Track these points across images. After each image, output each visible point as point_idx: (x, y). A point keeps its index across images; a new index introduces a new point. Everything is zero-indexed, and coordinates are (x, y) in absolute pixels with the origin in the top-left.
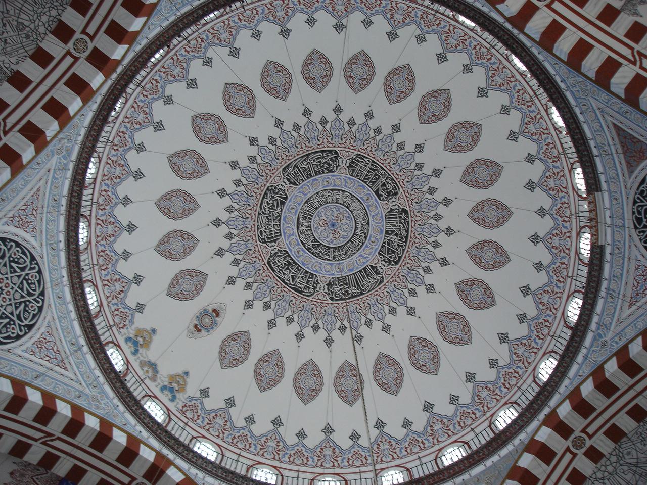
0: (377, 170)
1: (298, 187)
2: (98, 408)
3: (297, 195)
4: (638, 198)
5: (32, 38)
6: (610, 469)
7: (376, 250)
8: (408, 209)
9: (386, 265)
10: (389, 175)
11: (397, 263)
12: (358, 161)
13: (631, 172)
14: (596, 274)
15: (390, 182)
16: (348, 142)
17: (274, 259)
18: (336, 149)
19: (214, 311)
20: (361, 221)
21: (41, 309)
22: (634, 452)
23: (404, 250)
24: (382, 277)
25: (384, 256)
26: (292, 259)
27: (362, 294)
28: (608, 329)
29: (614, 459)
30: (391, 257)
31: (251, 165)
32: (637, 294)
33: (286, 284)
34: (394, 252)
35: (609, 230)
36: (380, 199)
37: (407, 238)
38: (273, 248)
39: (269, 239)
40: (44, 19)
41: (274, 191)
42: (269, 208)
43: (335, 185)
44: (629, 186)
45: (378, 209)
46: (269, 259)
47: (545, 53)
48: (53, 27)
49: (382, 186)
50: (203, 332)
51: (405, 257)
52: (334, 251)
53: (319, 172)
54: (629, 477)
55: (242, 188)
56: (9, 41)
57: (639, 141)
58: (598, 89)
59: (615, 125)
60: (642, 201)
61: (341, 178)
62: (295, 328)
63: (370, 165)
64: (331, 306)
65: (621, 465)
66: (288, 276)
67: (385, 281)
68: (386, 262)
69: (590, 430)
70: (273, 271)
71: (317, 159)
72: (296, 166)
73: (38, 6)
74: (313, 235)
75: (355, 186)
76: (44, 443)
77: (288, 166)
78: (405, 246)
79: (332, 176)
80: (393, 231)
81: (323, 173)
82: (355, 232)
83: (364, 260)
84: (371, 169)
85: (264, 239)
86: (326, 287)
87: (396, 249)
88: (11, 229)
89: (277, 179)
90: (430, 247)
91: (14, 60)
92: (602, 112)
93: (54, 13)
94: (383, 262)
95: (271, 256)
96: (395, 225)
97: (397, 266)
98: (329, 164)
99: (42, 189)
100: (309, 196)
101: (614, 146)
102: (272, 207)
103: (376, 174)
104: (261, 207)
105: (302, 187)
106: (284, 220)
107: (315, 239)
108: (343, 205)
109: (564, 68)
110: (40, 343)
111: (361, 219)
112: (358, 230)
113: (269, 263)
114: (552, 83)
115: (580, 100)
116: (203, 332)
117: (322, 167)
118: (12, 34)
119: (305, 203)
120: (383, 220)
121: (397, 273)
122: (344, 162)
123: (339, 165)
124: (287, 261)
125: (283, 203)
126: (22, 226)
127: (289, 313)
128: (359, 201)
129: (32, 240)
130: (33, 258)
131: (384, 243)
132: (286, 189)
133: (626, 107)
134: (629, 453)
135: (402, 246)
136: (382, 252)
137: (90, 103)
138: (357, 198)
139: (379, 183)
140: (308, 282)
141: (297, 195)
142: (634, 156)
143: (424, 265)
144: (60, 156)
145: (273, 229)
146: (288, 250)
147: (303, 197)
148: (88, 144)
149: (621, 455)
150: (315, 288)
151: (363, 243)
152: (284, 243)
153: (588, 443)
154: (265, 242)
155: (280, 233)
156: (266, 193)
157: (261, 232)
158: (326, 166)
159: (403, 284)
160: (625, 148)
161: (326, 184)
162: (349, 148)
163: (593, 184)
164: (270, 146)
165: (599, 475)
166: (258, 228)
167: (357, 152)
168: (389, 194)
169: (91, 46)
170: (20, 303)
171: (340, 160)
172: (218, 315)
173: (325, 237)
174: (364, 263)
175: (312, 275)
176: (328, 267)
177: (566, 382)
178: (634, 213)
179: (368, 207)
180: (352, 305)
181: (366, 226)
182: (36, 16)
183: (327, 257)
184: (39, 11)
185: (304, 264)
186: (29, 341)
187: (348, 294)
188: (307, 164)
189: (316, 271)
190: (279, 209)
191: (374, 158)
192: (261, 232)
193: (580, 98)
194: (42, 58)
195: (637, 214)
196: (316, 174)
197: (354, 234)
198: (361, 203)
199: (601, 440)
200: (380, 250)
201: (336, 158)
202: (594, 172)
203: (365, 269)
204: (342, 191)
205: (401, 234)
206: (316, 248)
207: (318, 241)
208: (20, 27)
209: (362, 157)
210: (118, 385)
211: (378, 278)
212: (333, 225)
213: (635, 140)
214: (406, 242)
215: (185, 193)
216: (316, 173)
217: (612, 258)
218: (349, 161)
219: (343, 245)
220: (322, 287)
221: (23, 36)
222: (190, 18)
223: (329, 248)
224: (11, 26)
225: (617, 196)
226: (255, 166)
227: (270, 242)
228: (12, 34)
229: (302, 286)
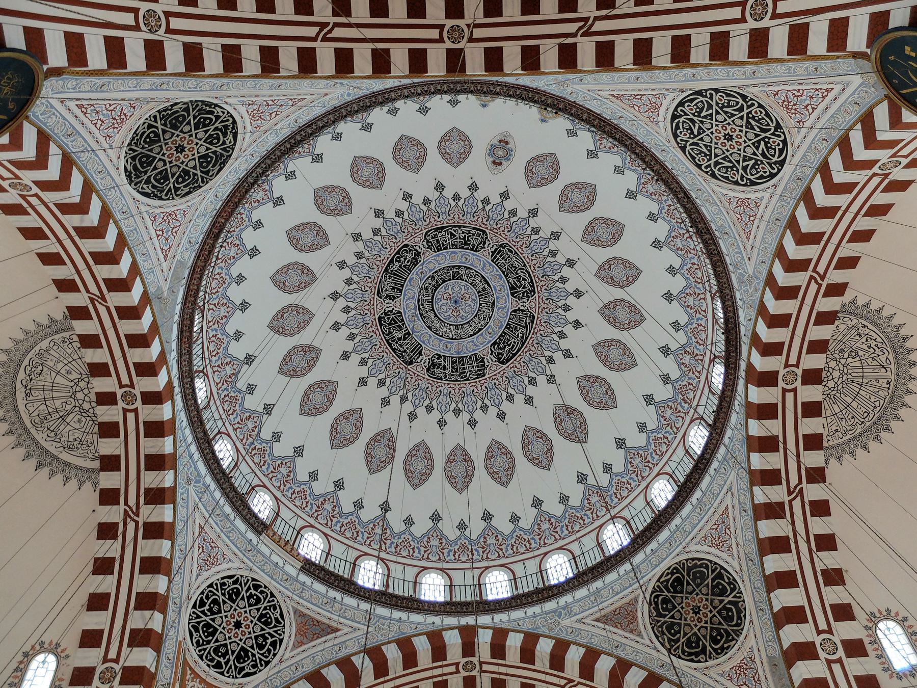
0: (459, 376)
1: (510, 311)
3: (505, 304)
4: (273, 601)
5: (837, 352)
6: (80, 396)
7: (405, 313)
8: (409, 367)
9: (387, 309)
10: (447, 380)
11: (380, 318)
12: (479, 370)
13: (296, 611)
14: (244, 513)
15: (440, 375)
16: (500, 380)
17: (482, 238)
18: (504, 366)
19: (500, 164)
20: (437, 324)
21: (675, 136)
22: (77, 426)
23: (383, 333)
24: (381, 298)
25: (394, 314)
26: (467, 249)
27: (386, 270)
28: (197, 493)
29: (86, 406)
30: (388, 318)
31: (564, 302)
32: (205, 540)
33: (455, 226)
34: (389, 324)
35: (267, 552)
36: (437, 354)
37: (390, 345)
38: (491, 246)
39: (500, 251)
40: (836, 374)
41: (528, 293)
42: (520, 276)
43: (482, 335)
44: (287, 600)
45: (432, 346)
46: (487, 235)
47: (430, 628)
48: (824, 373)
49: (445, 366)
50: (496, 142)
51: (377, 329)
52: (437, 282)
53: (503, 336)
54: (58, 403)
55: (556, 278)
56: (857, 337)
57: (312, 640)
58: (373, 643)
59: (338, 630)
60: (269, 602)
61: (481, 345)
63: (468, 375)
64: (402, 239)
65: (75, 406)
66: (459, 233)
67: (376, 296)
68: (389, 311)
70: (474, 229)
71: (513, 346)
72: (526, 326)
73: (849, 380)
74: (466, 281)
75: (467, 347)
76: (586, 19)
77: (533, 322)
78: (385, 338)
79: (491, 341)
80: (405, 339)
81: (499, 338)
82: (434, 311)
83: (407, 297)
84: (464, 372)
85: (504, 248)
86: (419, 250)
87: (390, 328)
88: (753, 196)
89: (531, 305)
90: (366, 355)
91: (842, 327)
92: (355, 630)
93: (831, 384)
94: (391, 309)
95: (487, 238)
96: (407, 345)
97: (377, 317)
98: (501, 349)
99: (746, 240)
100: (496, 310)
101: (323, 615)
102: (518, 278)
103: (457, 371)
104: (529, 273)
105: (507, 312)
106: (500, 276)
107: (461, 279)
108: (462, 325)
109: (408, 631)
110: (656, 108)
111: (438, 325)
112: (432, 315)
113: (484, 232)
114: (404, 607)
115: (376, 619)
116: (496, 142)
117: (504, 342)
118: (858, 345)
119: (494, 302)
120: (420, 340)
121: (372, 311)
122: (490, 360)
123: (491, 354)
124: (469, 244)
125: (512, 288)
126: (743, 202)
128: (452, 339)
129: (725, 192)
130: (713, 175)
131: (403, 325)
132: (519, 302)
133: (342, 654)
134: (80, 421)
135: (387, 335)
136: (399, 316)
137: (750, 334)
138: (455, 339)
139: (449, 367)
140: (438, 241)
141: (505, 304)
142: (305, 625)
143: (358, 338)
144: (747, 275)
145: (503, 261)
146: (477, 253)
147: (499, 306)
148: (728, 291)
149: (84, 414)
150: (428, 242)
151: (419, 309)
152: (484, 256)
153: (121, 405)
154: (501, 246)
155: (495, 263)
156: (533, 286)
157: (511, 252)
158: (502, 345)
159: (360, 308)
160: (315, 623)
161: (490, 331)
162: (495, 375)
163: (308, 567)
164: (560, 329)
165: (82, 384)
166: (516, 252)
167: (487, 376)
168: (434, 365)
169: (781, 384)
170: (699, 134)
171: (494, 360)
172: (494, 162)
173: (454, 287)
174: (405, 295)
175: (439, 250)
176: (431, 266)
177: (185, 423)
178: (265, 587)
179: (441, 341)
180: (387, 255)
181: (429, 323)
182: (846, 371)
183: (439, 274)
184: (845, 377)
185: (452, 252)
186: (668, 105)
187: (396, 261)
188: (518, 335)
189: (438, 255)
190: (511, 281)
191: (469, 383)
192: (511, 252)
193: (378, 621)
194: (818, 347)
195: (263, 589)
196: (503, 332)
197: (433, 310)
198: (449, 339)
199: (114, 415)
200: (401, 316)
201: (499, 359)
202: (317, 576)
203: (401, 291)
204: (471, 335)
205: (397, 343)
206: (455, 273)
207: (457, 279)
208: (854, 354)
209: (479, 376)
210: (549, 101)
211: (384, 294)
212: (456, 302)
213: (315, 636)
214: (387, 341)
215: (604, 246)
216: (505, 333)
217: (246, 538)
218: (487, 364)
219: (434, 294)
221: (846, 350)
222: (712, 447)
223: (444, 282)
224: (862, 350)
225: (287, 584)
226: (560, 304)
227: (496, 250)
228: (858, 345)
229: (440, 235)
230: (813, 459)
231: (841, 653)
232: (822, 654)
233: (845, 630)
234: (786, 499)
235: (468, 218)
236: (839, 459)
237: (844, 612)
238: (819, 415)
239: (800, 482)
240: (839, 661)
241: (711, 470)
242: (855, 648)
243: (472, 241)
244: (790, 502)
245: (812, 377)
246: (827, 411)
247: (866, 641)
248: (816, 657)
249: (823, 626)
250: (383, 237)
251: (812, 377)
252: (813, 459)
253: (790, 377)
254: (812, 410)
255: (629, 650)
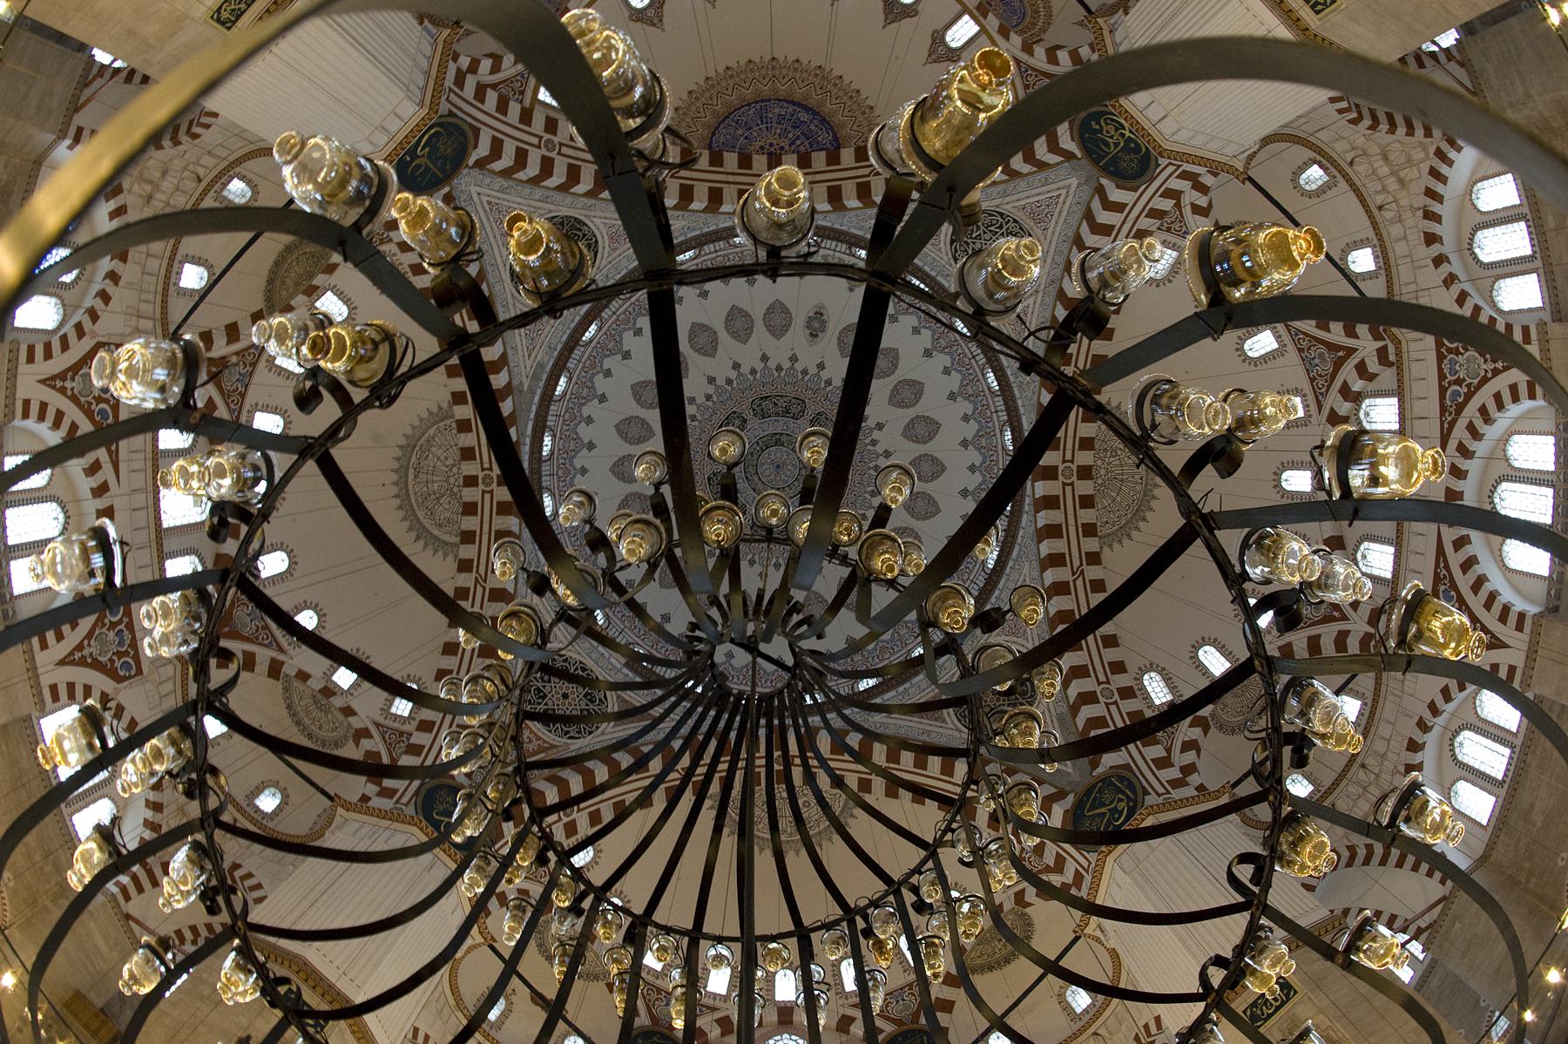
2: (856, 215)
11: (709, 479)
62: (745, 369)
69: (487, 496)
127: (758, 376)
176: (756, 433)
220: (749, 415)
230: (1091, 545)
231: (1116, 697)
232: (1102, 699)
233: (1121, 680)
234: (1071, 579)
235: (789, 388)
236: (1110, 546)
237: (1118, 667)
238: (1093, 507)
239: (1081, 565)
240: (1116, 703)
241: (1008, 570)
242: (1127, 693)
243: (793, 410)
244: (1074, 581)
245: (1085, 473)
246: (1101, 502)
247: (1136, 688)
248: (1096, 701)
249: (1102, 678)
250: (714, 403)
251: (1085, 473)
252: (1091, 545)
253: (1067, 473)
254: (1087, 502)
255: (933, 735)
